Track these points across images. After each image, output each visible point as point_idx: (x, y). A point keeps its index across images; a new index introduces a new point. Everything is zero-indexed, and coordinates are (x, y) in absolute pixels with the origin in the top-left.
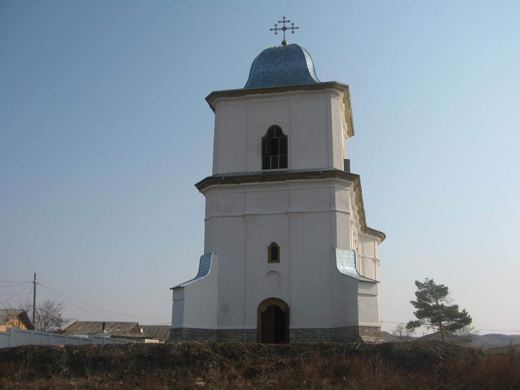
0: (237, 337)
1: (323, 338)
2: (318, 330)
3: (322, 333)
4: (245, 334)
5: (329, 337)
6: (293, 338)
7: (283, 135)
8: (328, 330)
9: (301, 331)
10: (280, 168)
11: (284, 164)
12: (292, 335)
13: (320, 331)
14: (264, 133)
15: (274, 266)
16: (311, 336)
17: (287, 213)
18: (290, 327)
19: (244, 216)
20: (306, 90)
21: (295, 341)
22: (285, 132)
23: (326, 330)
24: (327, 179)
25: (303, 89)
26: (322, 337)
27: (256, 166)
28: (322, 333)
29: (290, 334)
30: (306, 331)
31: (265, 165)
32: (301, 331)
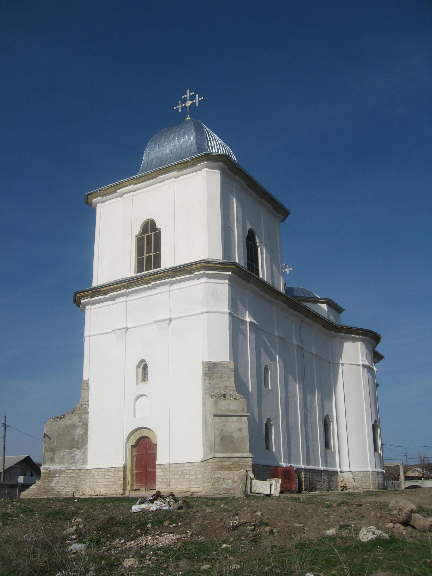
0: (106, 477)
1: (192, 475)
2: (186, 465)
4: (112, 474)
5: (198, 473)
6: (160, 476)
7: (157, 229)
8: (197, 464)
9: (168, 467)
10: (154, 269)
11: (158, 264)
12: (159, 472)
13: (189, 465)
14: (137, 230)
15: (143, 388)
16: (179, 473)
17: (156, 322)
18: (157, 463)
19: (113, 331)
20: (179, 170)
21: (163, 479)
22: (158, 226)
24: (195, 273)
25: (174, 170)
26: (192, 473)
27: (129, 270)
28: (191, 468)
29: (157, 470)
30: (174, 466)
31: (140, 268)
32: (168, 467)
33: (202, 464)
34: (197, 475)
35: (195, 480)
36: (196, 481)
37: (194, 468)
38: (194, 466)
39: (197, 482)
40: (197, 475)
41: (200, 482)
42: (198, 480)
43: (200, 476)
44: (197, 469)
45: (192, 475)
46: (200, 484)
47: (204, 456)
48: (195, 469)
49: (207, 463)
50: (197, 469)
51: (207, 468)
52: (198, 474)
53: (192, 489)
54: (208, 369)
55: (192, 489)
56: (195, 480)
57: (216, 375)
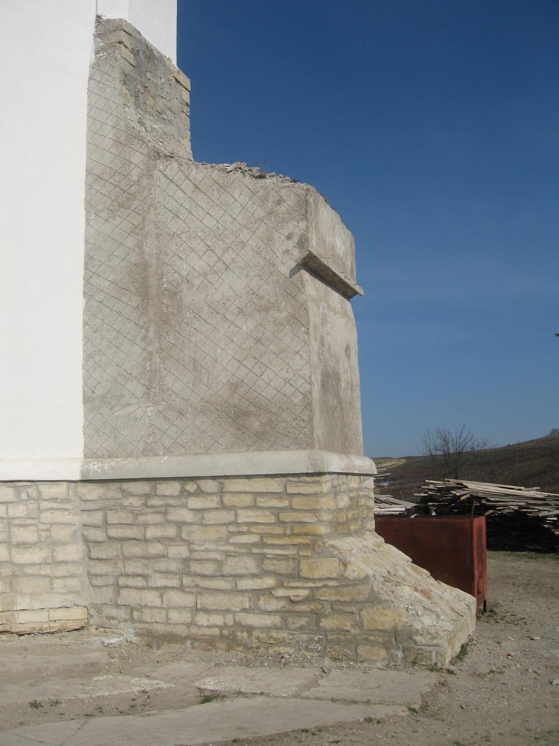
1: (24, 545)
3: (19, 511)
8: (60, 490)
23: (48, 491)
28: (19, 511)
33: (94, 492)
34: (55, 544)
35: (46, 571)
36: (52, 578)
37: (41, 511)
38: (40, 498)
39: (58, 583)
40: (55, 544)
41: (73, 583)
42: (61, 571)
43: (74, 552)
44: (59, 517)
45: (24, 545)
46: (77, 593)
47: (90, 455)
48: (47, 517)
49: (199, 493)
50: (59, 517)
51: (186, 515)
52: (64, 544)
53: (23, 617)
54: (131, 57)
55: (23, 617)
56: (46, 571)
57: (151, 102)
